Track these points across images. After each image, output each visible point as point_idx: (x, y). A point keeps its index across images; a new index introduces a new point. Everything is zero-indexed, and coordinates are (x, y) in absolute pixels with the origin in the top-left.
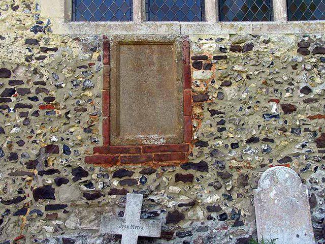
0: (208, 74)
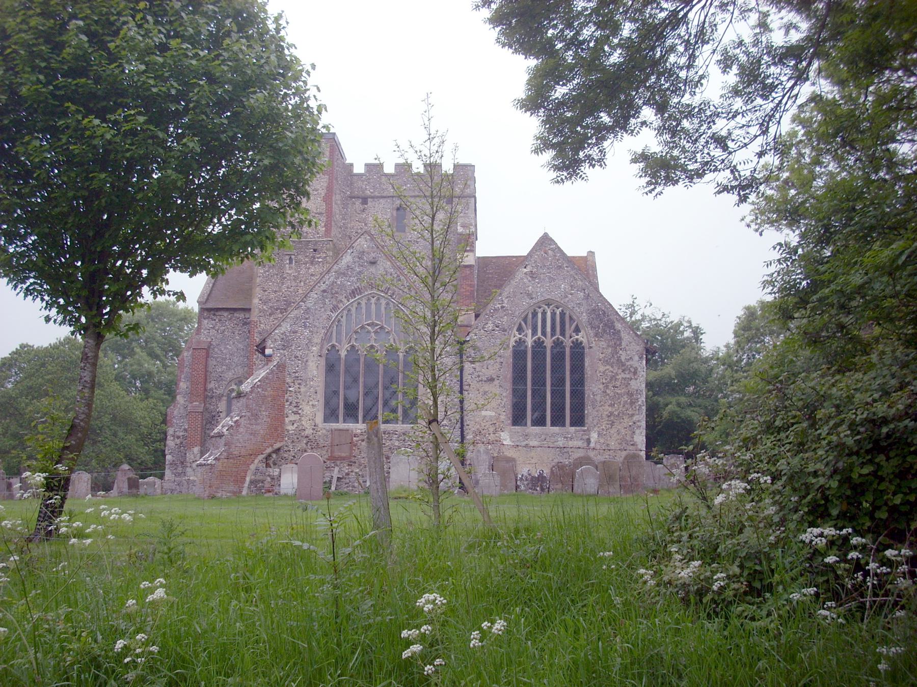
0: (358, 439)
